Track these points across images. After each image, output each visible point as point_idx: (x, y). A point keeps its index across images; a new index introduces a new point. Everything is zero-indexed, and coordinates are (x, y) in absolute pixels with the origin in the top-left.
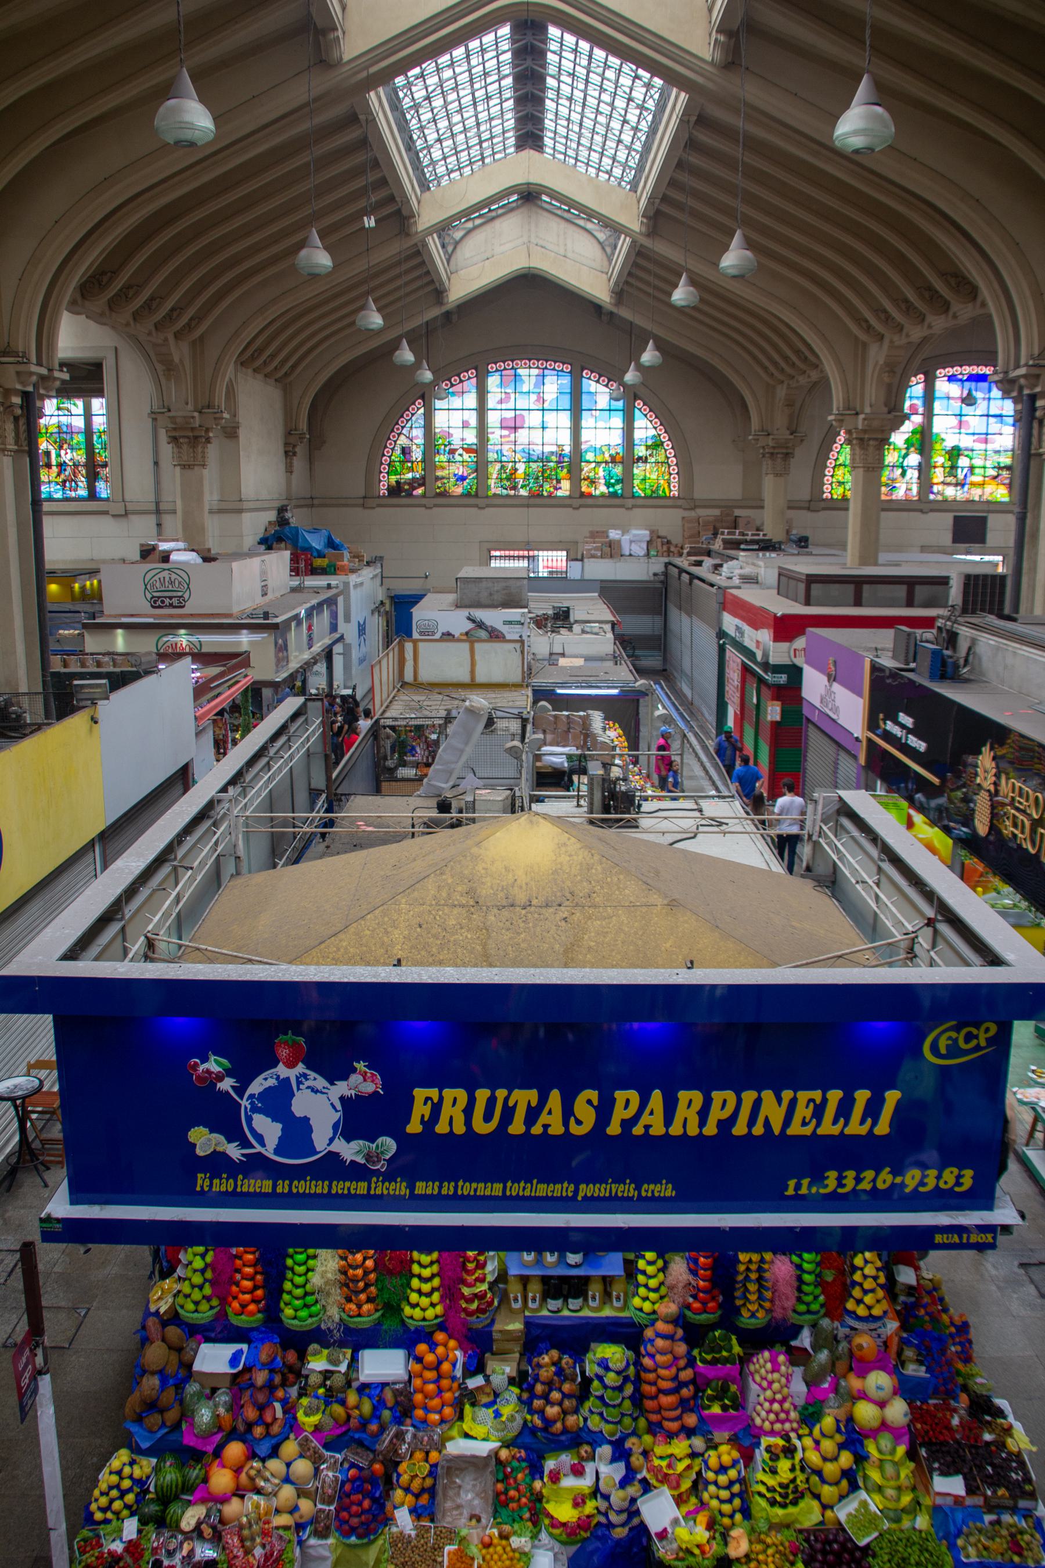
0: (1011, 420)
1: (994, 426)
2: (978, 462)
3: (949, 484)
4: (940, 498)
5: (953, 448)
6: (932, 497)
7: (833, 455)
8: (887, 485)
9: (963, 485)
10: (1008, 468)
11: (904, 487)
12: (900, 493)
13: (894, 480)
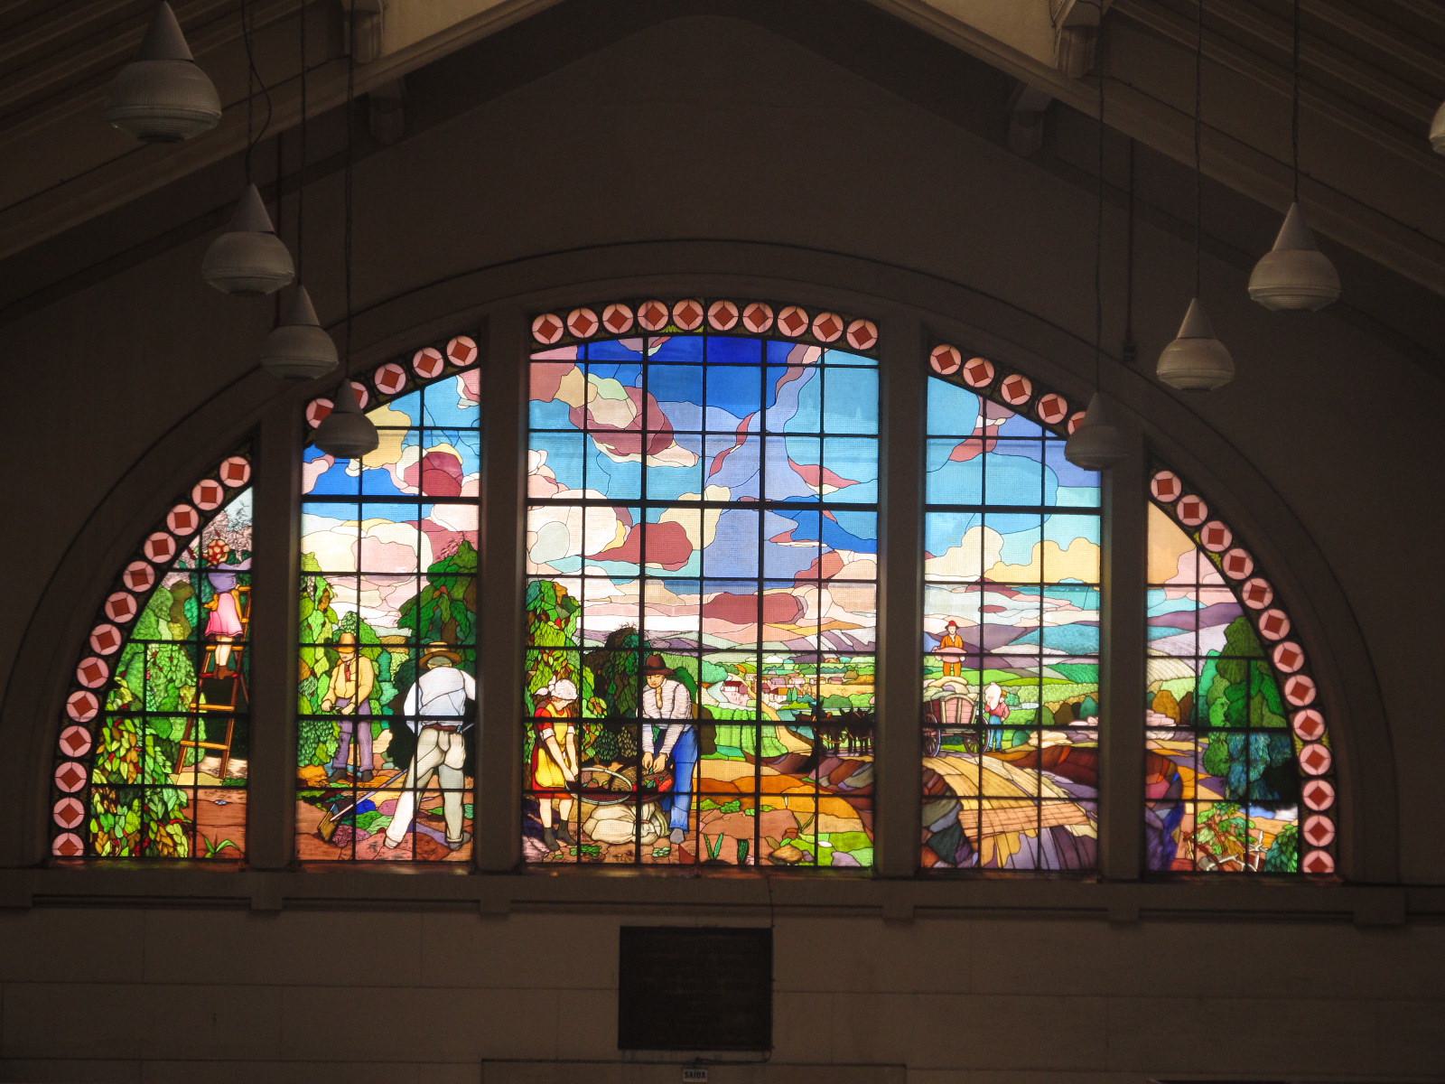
0: (865, 525)
1: (791, 552)
2: (720, 701)
3: (604, 794)
4: (567, 853)
5: (618, 640)
8: (327, 797)
9: (665, 800)
10: (855, 722)
11: (406, 803)
13: (360, 778)
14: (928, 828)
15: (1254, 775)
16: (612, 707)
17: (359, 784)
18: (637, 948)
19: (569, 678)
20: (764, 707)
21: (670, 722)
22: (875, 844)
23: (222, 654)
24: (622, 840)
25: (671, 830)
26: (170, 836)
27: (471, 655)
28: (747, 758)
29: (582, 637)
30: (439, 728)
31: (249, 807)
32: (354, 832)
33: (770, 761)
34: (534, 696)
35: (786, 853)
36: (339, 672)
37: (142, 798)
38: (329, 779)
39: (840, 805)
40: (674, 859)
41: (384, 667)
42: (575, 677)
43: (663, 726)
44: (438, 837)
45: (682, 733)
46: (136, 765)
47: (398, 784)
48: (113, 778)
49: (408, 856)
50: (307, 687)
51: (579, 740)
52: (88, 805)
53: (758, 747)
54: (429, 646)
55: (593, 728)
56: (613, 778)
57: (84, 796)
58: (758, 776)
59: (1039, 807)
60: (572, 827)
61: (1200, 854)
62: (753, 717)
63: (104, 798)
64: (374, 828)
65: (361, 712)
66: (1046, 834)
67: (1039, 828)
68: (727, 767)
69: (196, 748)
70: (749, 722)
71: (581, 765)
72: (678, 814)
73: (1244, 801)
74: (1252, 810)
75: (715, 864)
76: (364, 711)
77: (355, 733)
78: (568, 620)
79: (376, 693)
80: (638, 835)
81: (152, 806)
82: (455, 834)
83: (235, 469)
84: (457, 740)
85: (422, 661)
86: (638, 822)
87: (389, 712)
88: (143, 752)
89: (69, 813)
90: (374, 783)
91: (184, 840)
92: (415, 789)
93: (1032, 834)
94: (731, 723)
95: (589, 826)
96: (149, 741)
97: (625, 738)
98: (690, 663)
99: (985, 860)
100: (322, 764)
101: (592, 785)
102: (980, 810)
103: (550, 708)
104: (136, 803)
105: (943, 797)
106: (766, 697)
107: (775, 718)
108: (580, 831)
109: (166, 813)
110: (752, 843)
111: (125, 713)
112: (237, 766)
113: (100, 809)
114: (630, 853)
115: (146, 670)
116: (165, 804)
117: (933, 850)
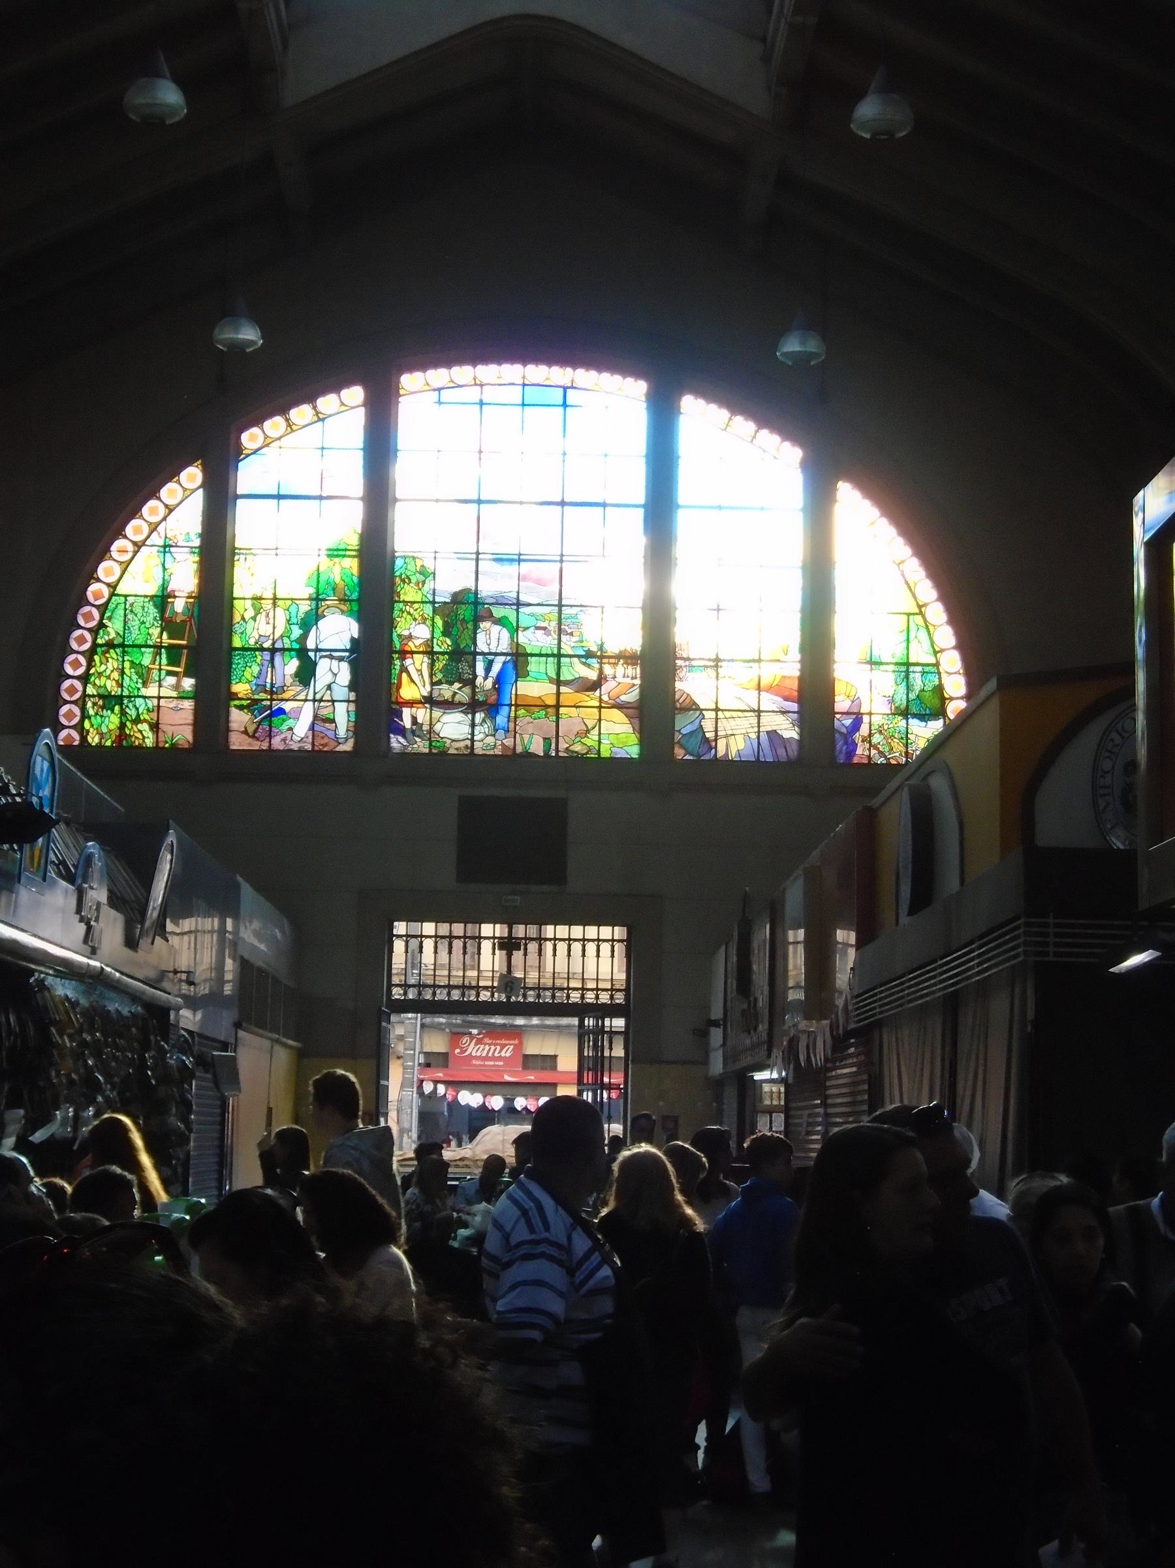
2: (531, 640)
3: (448, 705)
4: (421, 746)
5: (458, 598)
6: (396, 742)
7: (87, 617)
8: (252, 705)
9: (492, 709)
10: (628, 658)
12: (298, 728)
14: (679, 731)
15: (912, 696)
16: (456, 643)
17: (275, 697)
18: (470, 809)
19: (424, 623)
20: (563, 645)
21: (496, 654)
22: (642, 742)
23: (179, 605)
24: (461, 737)
25: (496, 730)
26: (141, 732)
27: (355, 607)
28: (551, 681)
29: (434, 594)
30: (331, 657)
31: (196, 712)
32: (270, 730)
33: (567, 683)
34: (399, 636)
35: (577, 748)
36: (261, 618)
37: (121, 704)
38: (253, 693)
39: (617, 714)
40: (498, 752)
41: (293, 614)
42: (429, 622)
43: (491, 657)
44: (331, 734)
45: (505, 663)
46: (117, 682)
47: (302, 697)
48: (102, 691)
49: (309, 747)
50: (237, 627)
51: (432, 666)
52: (83, 709)
53: (558, 674)
54: (325, 600)
55: (441, 657)
56: (455, 694)
57: (80, 703)
58: (558, 694)
59: (759, 716)
60: (426, 728)
61: (873, 752)
62: (555, 652)
63: (94, 704)
64: (284, 727)
65: (276, 646)
66: (764, 737)
67: (759, 732)
68: (535, 686)
69: (160, 670)
70: (553, 655)
71: (433, 684)
72: (501, 720)
73: (905, 713)
74: (910, 720)
75: (528, 755)
76: (278, 645)
77: (272, 661)
78: (424, 583)
79: (286, 635)
80: (473, 734)
81: (127, 710)
82: (342, 732)
83: (192, 475)
84: (345, 668)
85: (320, 611)
86: (473, 725)
87: (296, 646)
88: (122, 673)
89: (70, 715)
90: (285, 696)
91: (150, 735)
92: (314, 700)
93: (753, 736)
94: (540, 655)
95: (437, 727)
96: (127, 665)
97: (464, 667)
98: (510, 613)
99: (721, 751)
100: (249, 682)
101: (439, 699)
102: (717, 719)
103: (410, 644)
104: (117, 708)
105: (689, 709)
106: (563, 638)
107: (571, 652)
108: (430, 731)
109: (138, 715)
110: (554, 741)
111: (110, 645)
112: (188, 683)
113: (91, 712)
114: (466, 747)
115: (125, 615)
116: (137, 709)
117: (682, 746)
